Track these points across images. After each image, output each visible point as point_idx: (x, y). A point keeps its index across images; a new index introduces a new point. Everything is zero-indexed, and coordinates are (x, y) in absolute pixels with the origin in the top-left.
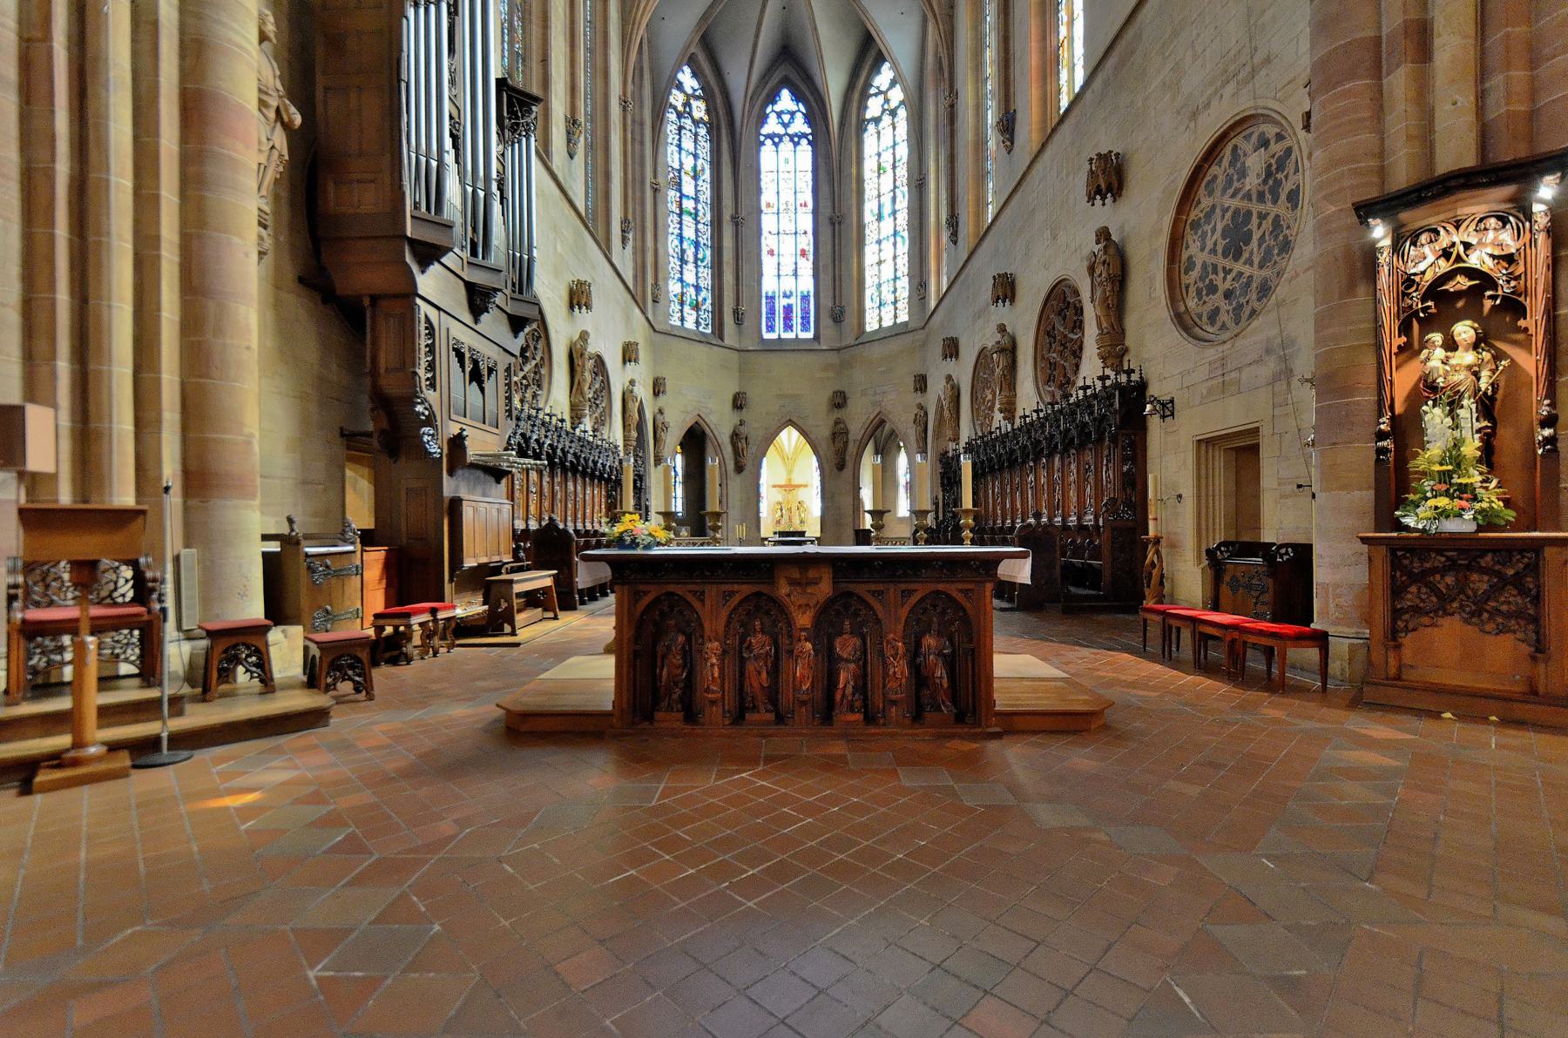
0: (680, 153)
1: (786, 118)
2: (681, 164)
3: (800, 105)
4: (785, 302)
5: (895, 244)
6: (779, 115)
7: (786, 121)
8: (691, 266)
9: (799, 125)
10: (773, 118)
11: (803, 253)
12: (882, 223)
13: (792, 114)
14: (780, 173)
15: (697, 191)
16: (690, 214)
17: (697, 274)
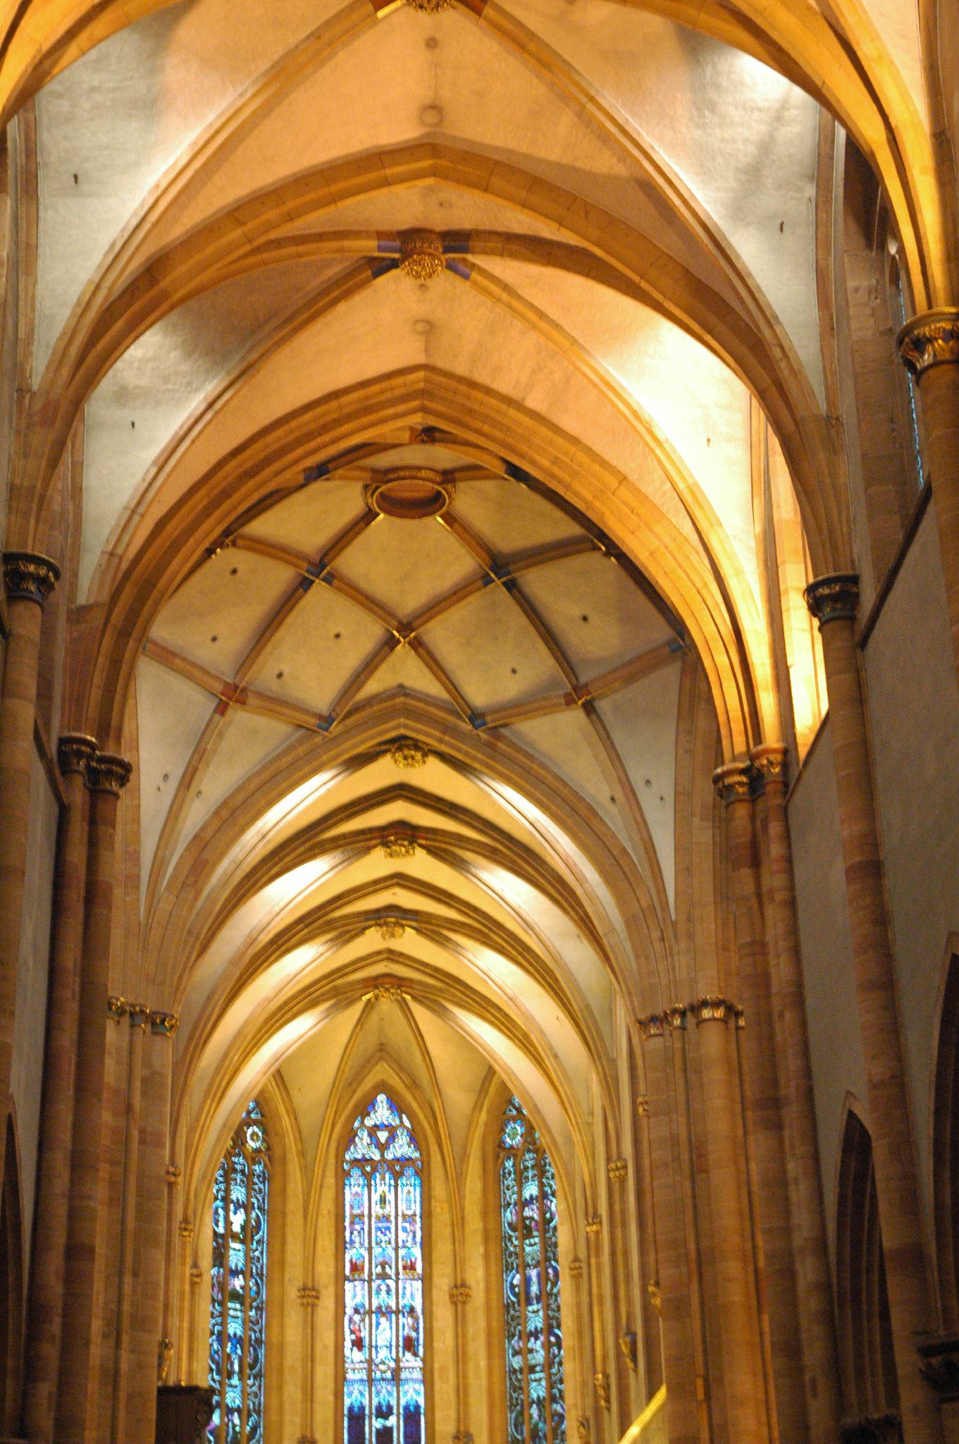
0: (226, 1209)
1: (383, 1136)
2: (228, 1223)
3: (404, 1117)
4: (378, 1424)
5: (547, 1346)
6: (373, 1131)
7: (383, 1140)
8: (235, 1381)
9: (402, 1148)
10: (363, 1139)
11: (409, 1345)
12: (530, 1308)
13: (392, 1130)
14: (373, 1220)
15: (249, 1259)
16: (235, 1296)
17: (243, 1391)
